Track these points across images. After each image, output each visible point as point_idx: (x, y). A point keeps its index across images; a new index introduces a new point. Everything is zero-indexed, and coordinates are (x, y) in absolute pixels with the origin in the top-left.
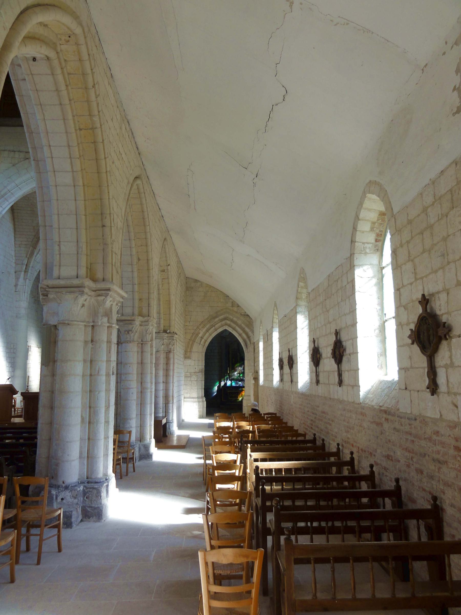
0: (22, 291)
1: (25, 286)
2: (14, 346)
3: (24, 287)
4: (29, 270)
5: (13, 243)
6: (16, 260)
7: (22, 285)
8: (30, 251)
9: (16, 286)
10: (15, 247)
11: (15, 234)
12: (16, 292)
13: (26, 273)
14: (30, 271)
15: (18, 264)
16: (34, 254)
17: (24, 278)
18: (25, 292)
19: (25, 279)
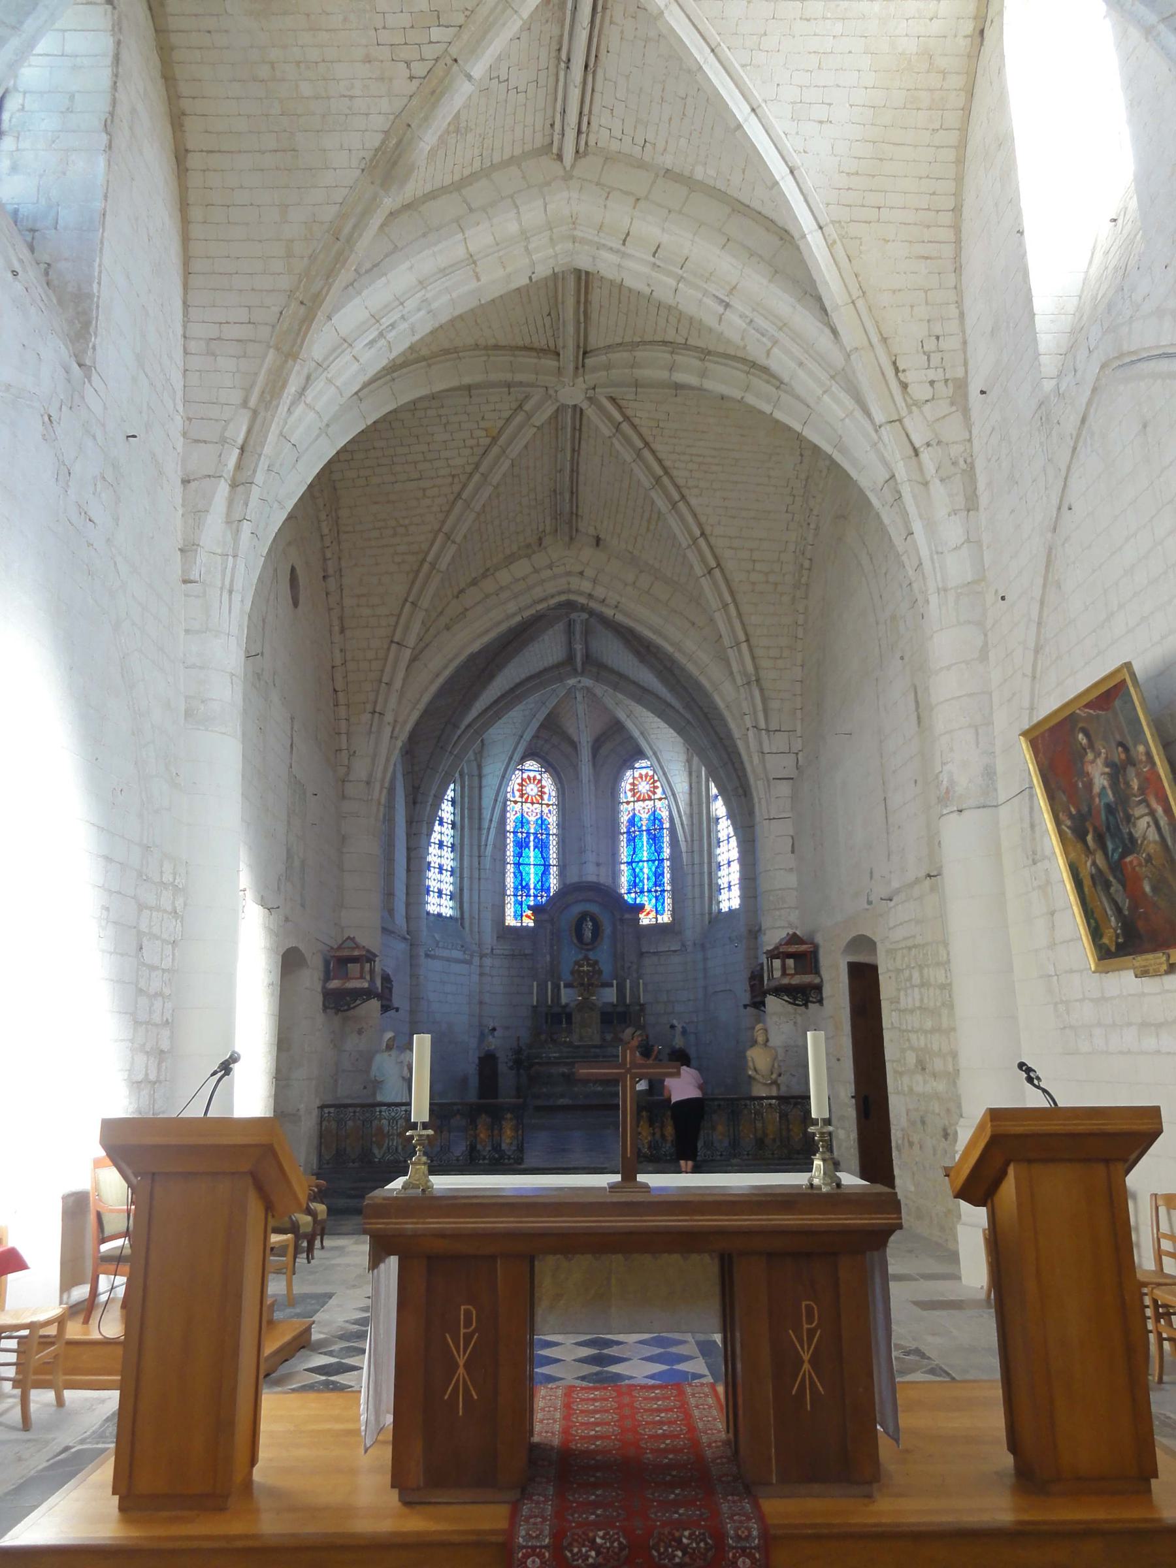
0: (219, 584)
1: (235, 556)
2: (175, 874)
3: (230, 565)
4: (255, 471)
5: (180, 331)
6: (189, 419)
7: (219, 551)
8: (263, 371)
9: (188, 549)
10: (186, 352)
11: (186, 287)
12: (185, 582)
13: (240, 489)
14: (259, 478)
15: (197, 441)
16: (284, 386)
17: (228, 514)
18: (231, 592)
19: (233, 522)
